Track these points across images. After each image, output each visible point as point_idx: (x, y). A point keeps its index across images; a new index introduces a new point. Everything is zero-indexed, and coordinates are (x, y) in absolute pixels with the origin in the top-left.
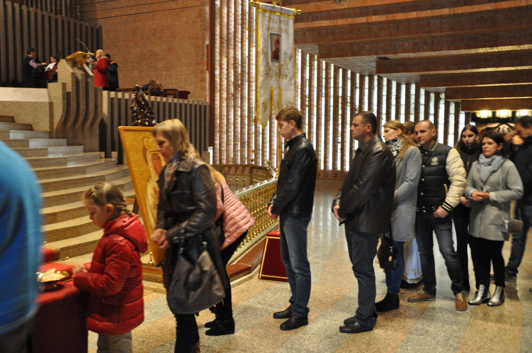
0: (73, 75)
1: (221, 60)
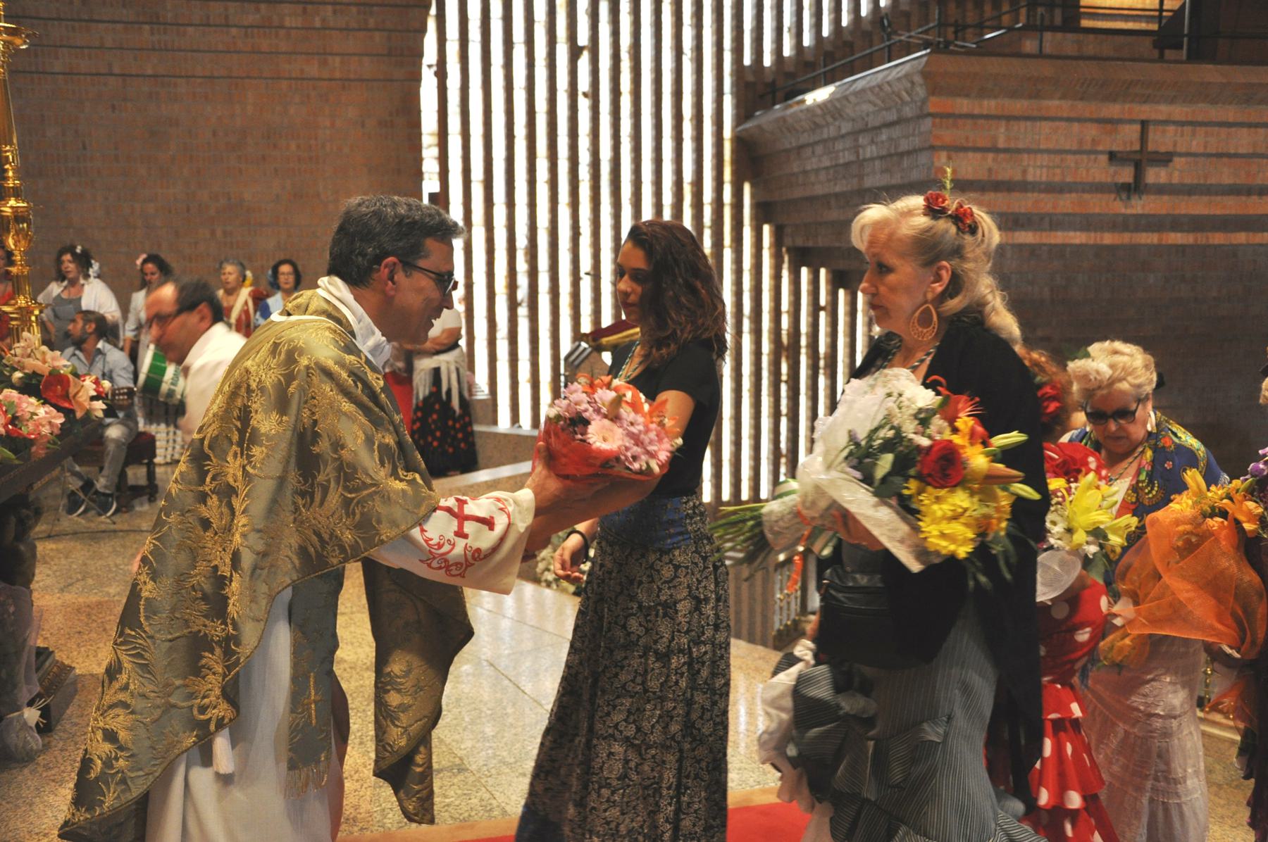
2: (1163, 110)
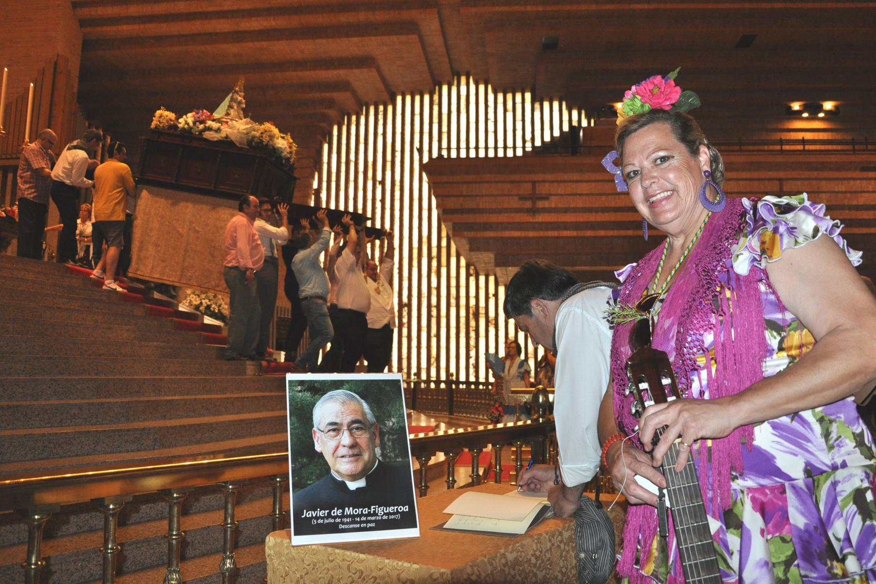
2: (540, 177)
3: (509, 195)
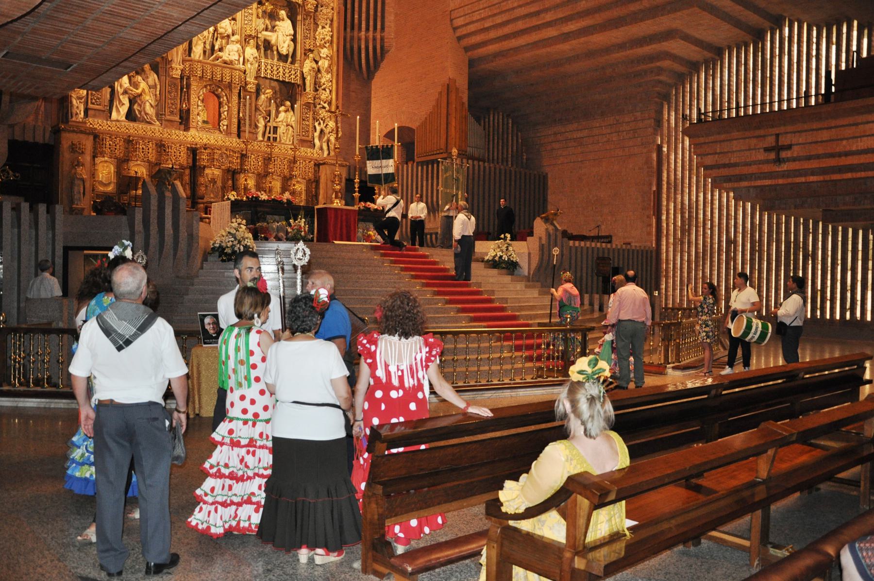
0: (547, 229)
1: (668, 205)
2: (782, 129)
3: (755, 149)
